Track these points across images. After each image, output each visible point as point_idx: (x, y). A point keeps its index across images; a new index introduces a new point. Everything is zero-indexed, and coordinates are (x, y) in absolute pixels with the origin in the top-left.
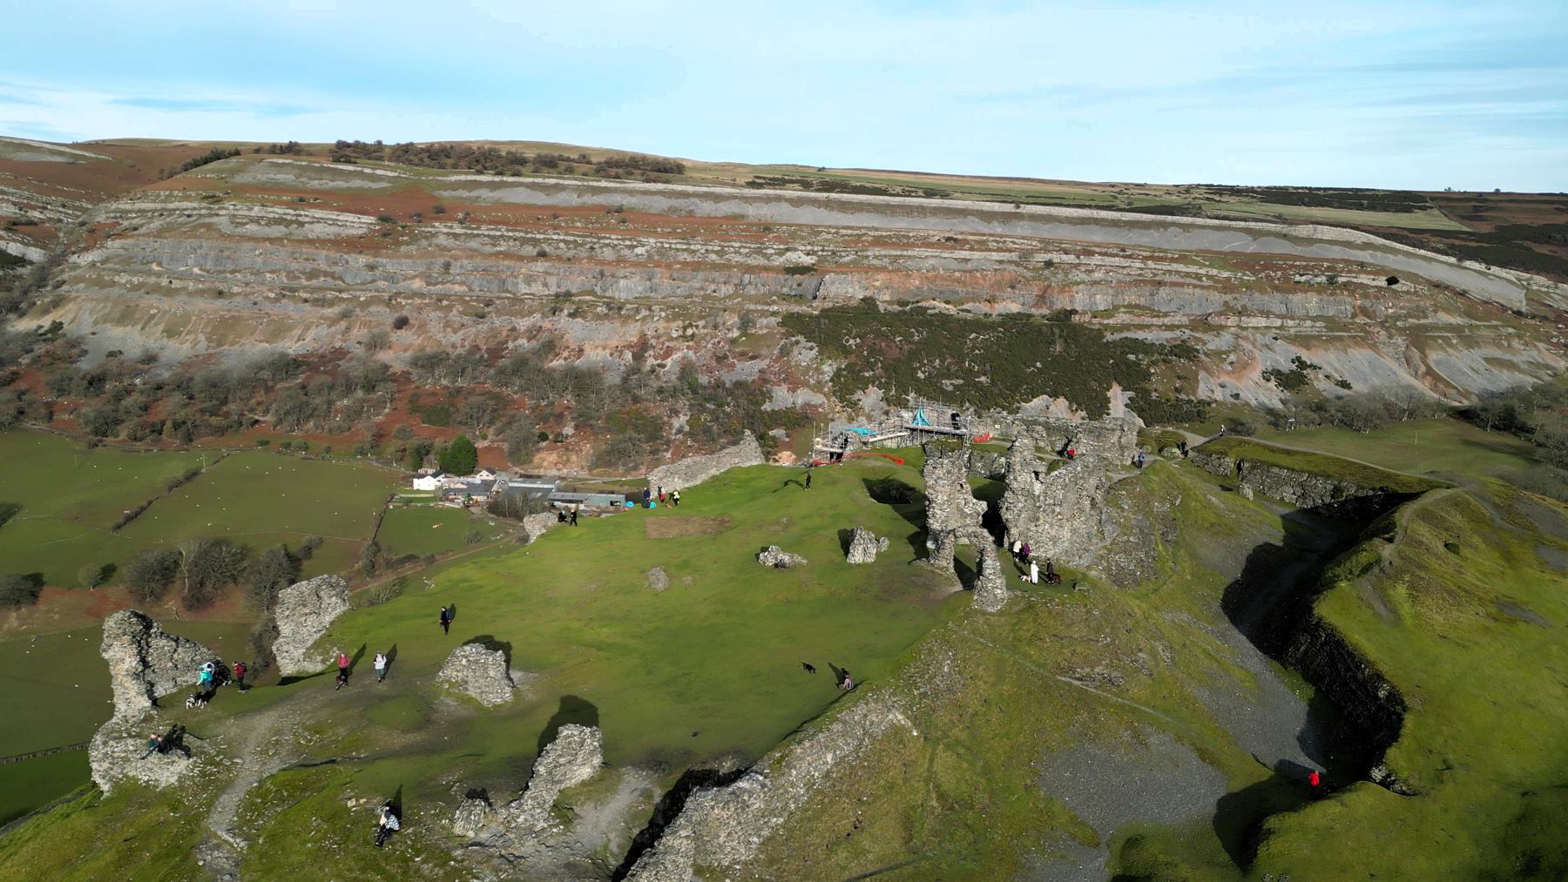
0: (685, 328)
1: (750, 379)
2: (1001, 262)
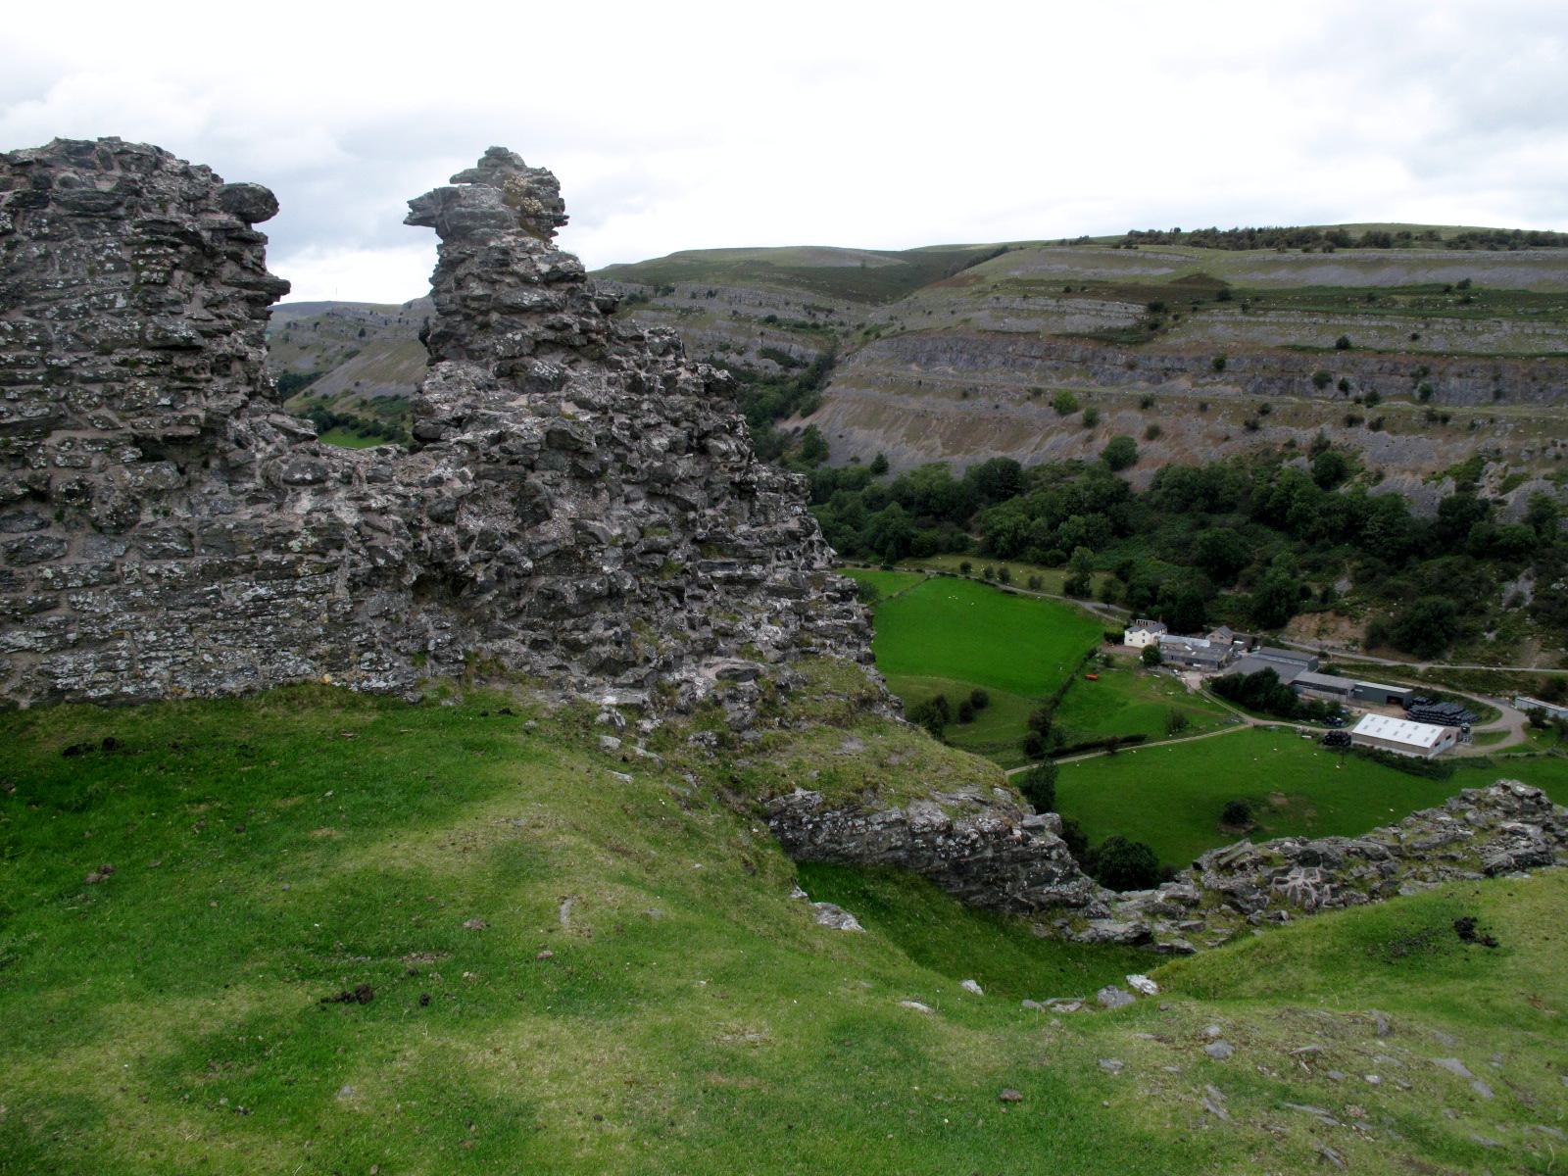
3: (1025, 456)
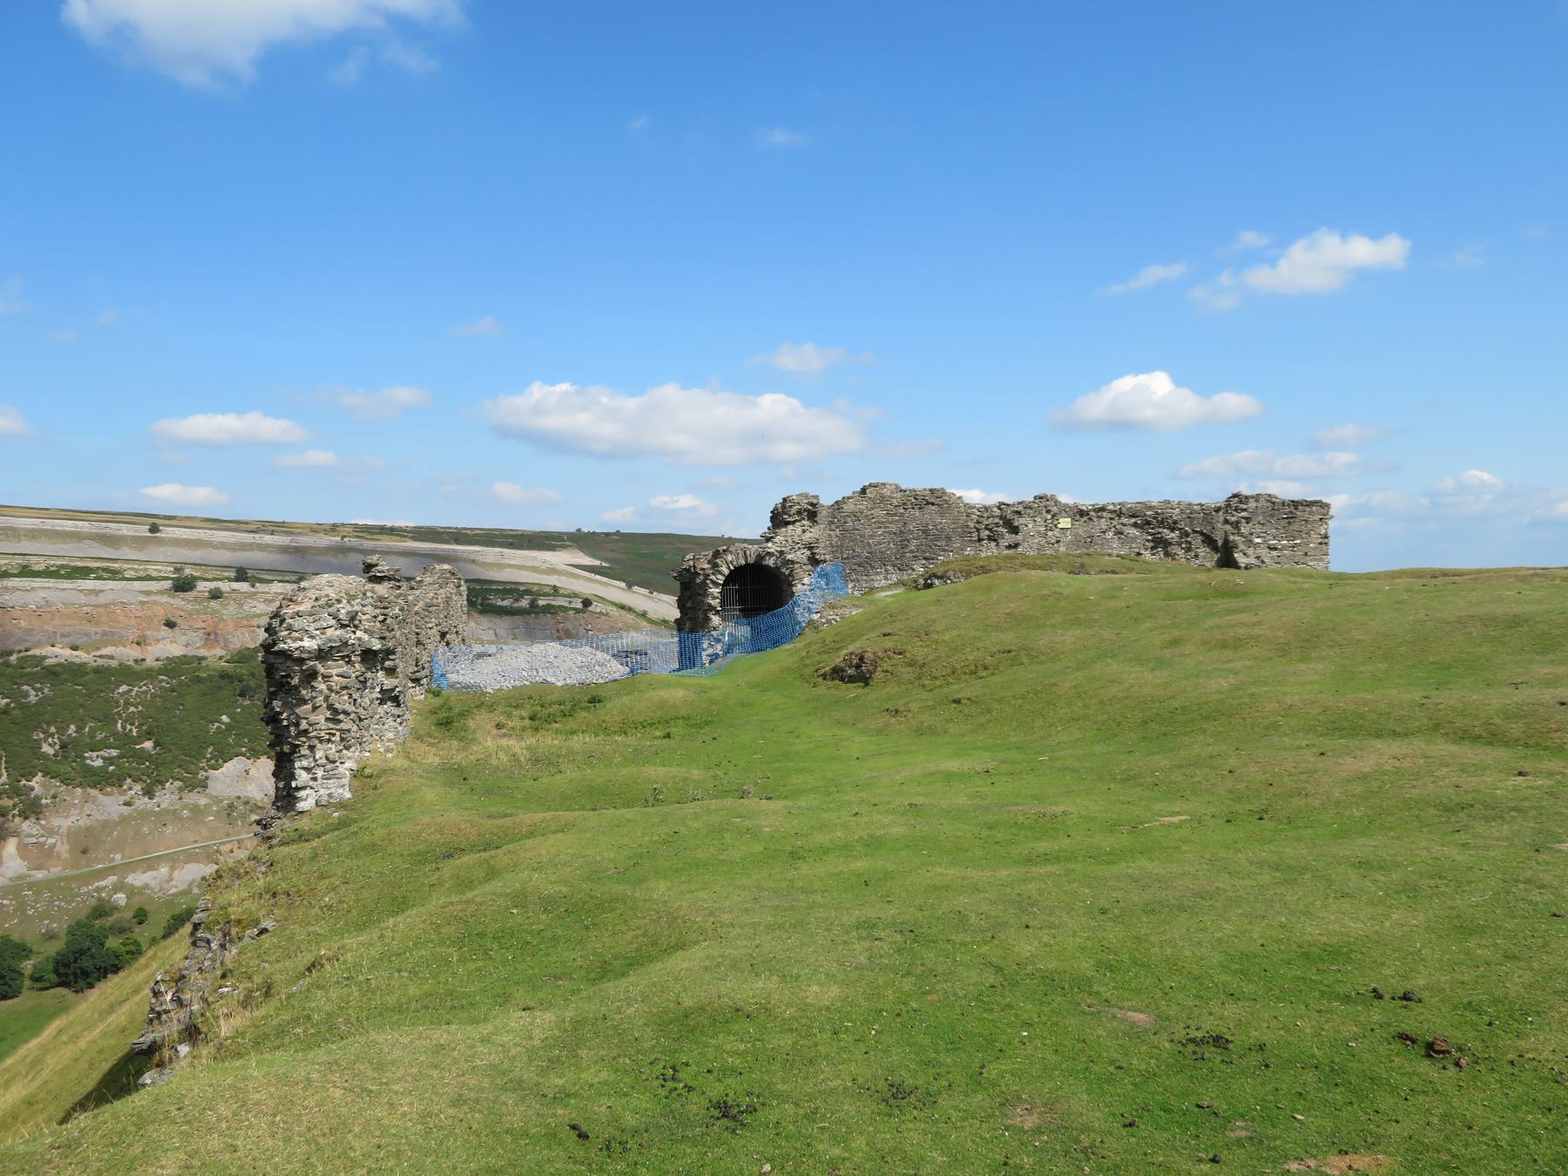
2: (148, 593)
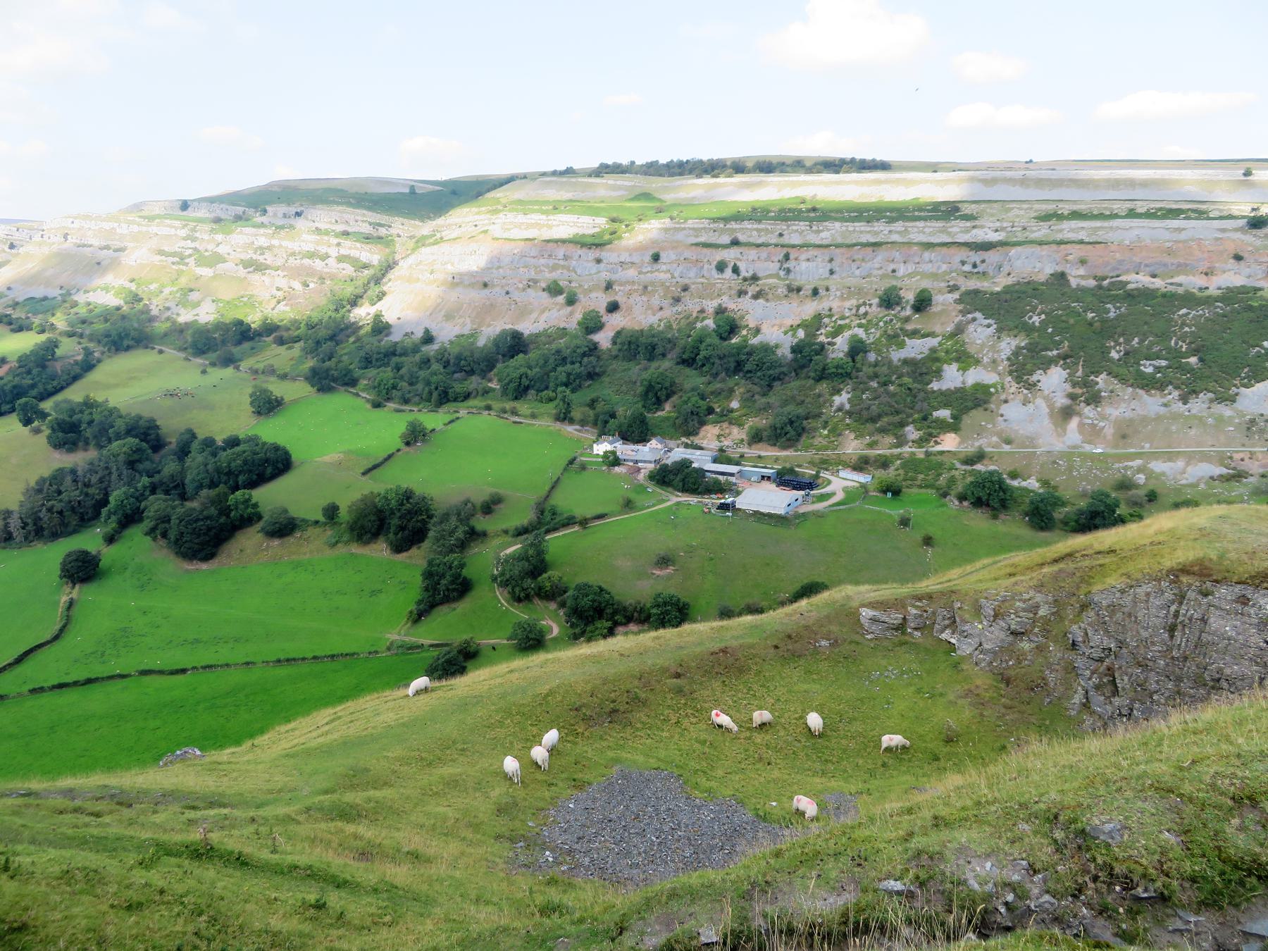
0: (858, 307)
1: (920, 357)
3: (527, 327)
